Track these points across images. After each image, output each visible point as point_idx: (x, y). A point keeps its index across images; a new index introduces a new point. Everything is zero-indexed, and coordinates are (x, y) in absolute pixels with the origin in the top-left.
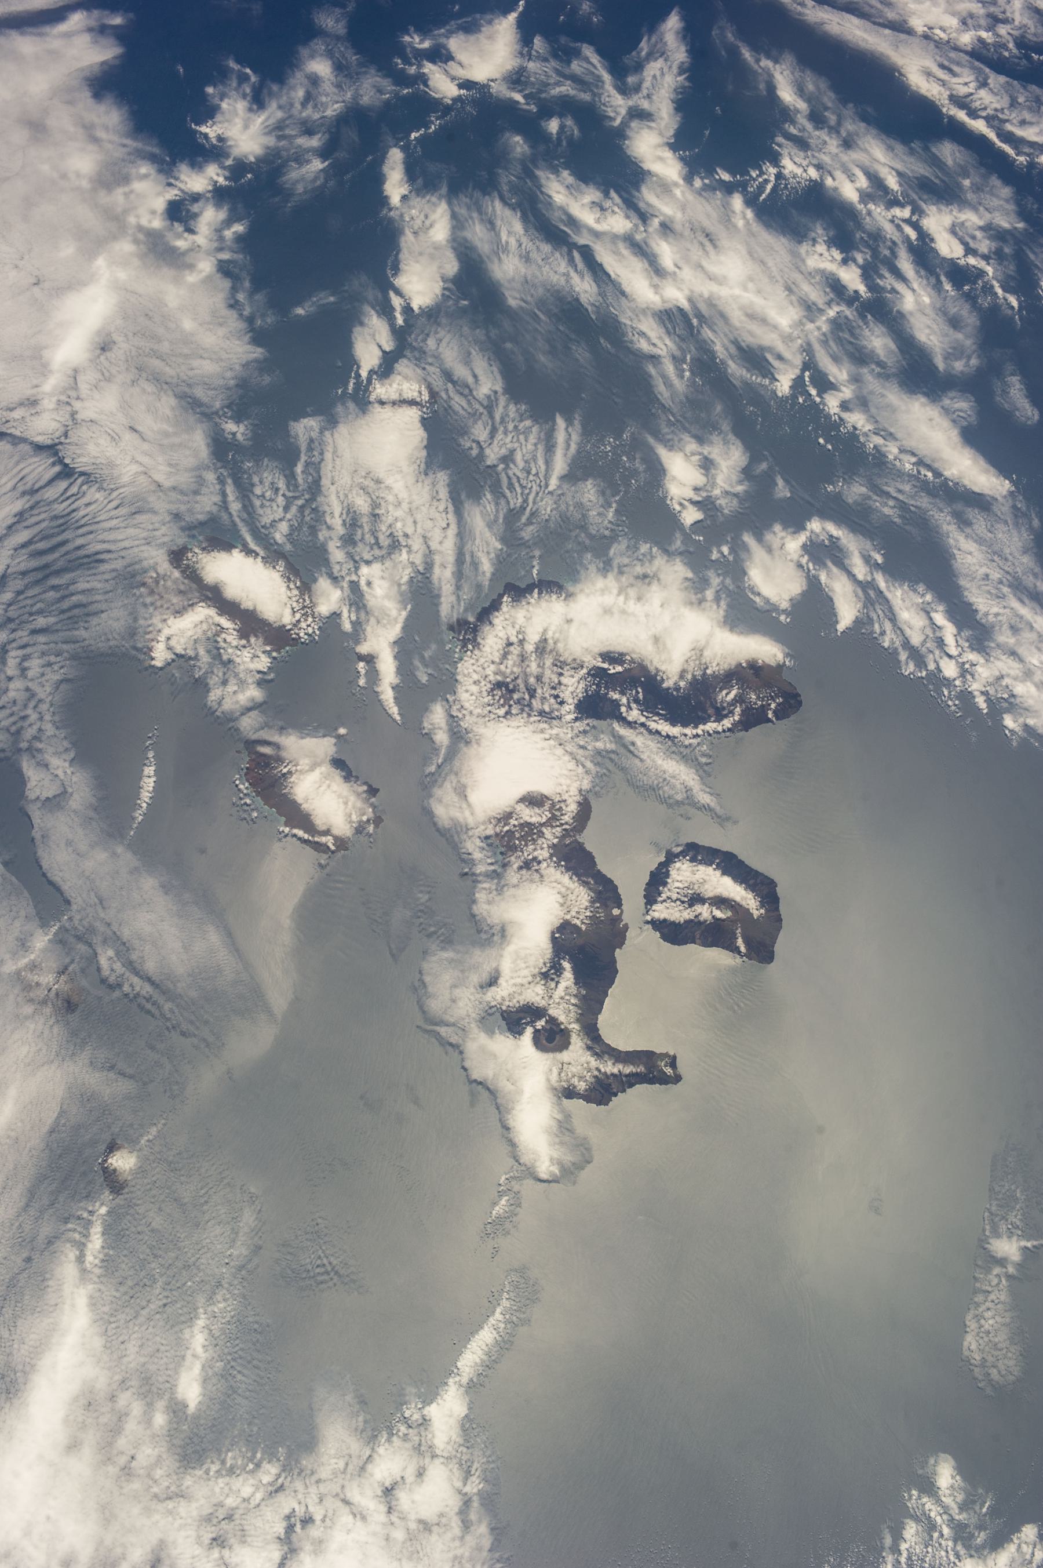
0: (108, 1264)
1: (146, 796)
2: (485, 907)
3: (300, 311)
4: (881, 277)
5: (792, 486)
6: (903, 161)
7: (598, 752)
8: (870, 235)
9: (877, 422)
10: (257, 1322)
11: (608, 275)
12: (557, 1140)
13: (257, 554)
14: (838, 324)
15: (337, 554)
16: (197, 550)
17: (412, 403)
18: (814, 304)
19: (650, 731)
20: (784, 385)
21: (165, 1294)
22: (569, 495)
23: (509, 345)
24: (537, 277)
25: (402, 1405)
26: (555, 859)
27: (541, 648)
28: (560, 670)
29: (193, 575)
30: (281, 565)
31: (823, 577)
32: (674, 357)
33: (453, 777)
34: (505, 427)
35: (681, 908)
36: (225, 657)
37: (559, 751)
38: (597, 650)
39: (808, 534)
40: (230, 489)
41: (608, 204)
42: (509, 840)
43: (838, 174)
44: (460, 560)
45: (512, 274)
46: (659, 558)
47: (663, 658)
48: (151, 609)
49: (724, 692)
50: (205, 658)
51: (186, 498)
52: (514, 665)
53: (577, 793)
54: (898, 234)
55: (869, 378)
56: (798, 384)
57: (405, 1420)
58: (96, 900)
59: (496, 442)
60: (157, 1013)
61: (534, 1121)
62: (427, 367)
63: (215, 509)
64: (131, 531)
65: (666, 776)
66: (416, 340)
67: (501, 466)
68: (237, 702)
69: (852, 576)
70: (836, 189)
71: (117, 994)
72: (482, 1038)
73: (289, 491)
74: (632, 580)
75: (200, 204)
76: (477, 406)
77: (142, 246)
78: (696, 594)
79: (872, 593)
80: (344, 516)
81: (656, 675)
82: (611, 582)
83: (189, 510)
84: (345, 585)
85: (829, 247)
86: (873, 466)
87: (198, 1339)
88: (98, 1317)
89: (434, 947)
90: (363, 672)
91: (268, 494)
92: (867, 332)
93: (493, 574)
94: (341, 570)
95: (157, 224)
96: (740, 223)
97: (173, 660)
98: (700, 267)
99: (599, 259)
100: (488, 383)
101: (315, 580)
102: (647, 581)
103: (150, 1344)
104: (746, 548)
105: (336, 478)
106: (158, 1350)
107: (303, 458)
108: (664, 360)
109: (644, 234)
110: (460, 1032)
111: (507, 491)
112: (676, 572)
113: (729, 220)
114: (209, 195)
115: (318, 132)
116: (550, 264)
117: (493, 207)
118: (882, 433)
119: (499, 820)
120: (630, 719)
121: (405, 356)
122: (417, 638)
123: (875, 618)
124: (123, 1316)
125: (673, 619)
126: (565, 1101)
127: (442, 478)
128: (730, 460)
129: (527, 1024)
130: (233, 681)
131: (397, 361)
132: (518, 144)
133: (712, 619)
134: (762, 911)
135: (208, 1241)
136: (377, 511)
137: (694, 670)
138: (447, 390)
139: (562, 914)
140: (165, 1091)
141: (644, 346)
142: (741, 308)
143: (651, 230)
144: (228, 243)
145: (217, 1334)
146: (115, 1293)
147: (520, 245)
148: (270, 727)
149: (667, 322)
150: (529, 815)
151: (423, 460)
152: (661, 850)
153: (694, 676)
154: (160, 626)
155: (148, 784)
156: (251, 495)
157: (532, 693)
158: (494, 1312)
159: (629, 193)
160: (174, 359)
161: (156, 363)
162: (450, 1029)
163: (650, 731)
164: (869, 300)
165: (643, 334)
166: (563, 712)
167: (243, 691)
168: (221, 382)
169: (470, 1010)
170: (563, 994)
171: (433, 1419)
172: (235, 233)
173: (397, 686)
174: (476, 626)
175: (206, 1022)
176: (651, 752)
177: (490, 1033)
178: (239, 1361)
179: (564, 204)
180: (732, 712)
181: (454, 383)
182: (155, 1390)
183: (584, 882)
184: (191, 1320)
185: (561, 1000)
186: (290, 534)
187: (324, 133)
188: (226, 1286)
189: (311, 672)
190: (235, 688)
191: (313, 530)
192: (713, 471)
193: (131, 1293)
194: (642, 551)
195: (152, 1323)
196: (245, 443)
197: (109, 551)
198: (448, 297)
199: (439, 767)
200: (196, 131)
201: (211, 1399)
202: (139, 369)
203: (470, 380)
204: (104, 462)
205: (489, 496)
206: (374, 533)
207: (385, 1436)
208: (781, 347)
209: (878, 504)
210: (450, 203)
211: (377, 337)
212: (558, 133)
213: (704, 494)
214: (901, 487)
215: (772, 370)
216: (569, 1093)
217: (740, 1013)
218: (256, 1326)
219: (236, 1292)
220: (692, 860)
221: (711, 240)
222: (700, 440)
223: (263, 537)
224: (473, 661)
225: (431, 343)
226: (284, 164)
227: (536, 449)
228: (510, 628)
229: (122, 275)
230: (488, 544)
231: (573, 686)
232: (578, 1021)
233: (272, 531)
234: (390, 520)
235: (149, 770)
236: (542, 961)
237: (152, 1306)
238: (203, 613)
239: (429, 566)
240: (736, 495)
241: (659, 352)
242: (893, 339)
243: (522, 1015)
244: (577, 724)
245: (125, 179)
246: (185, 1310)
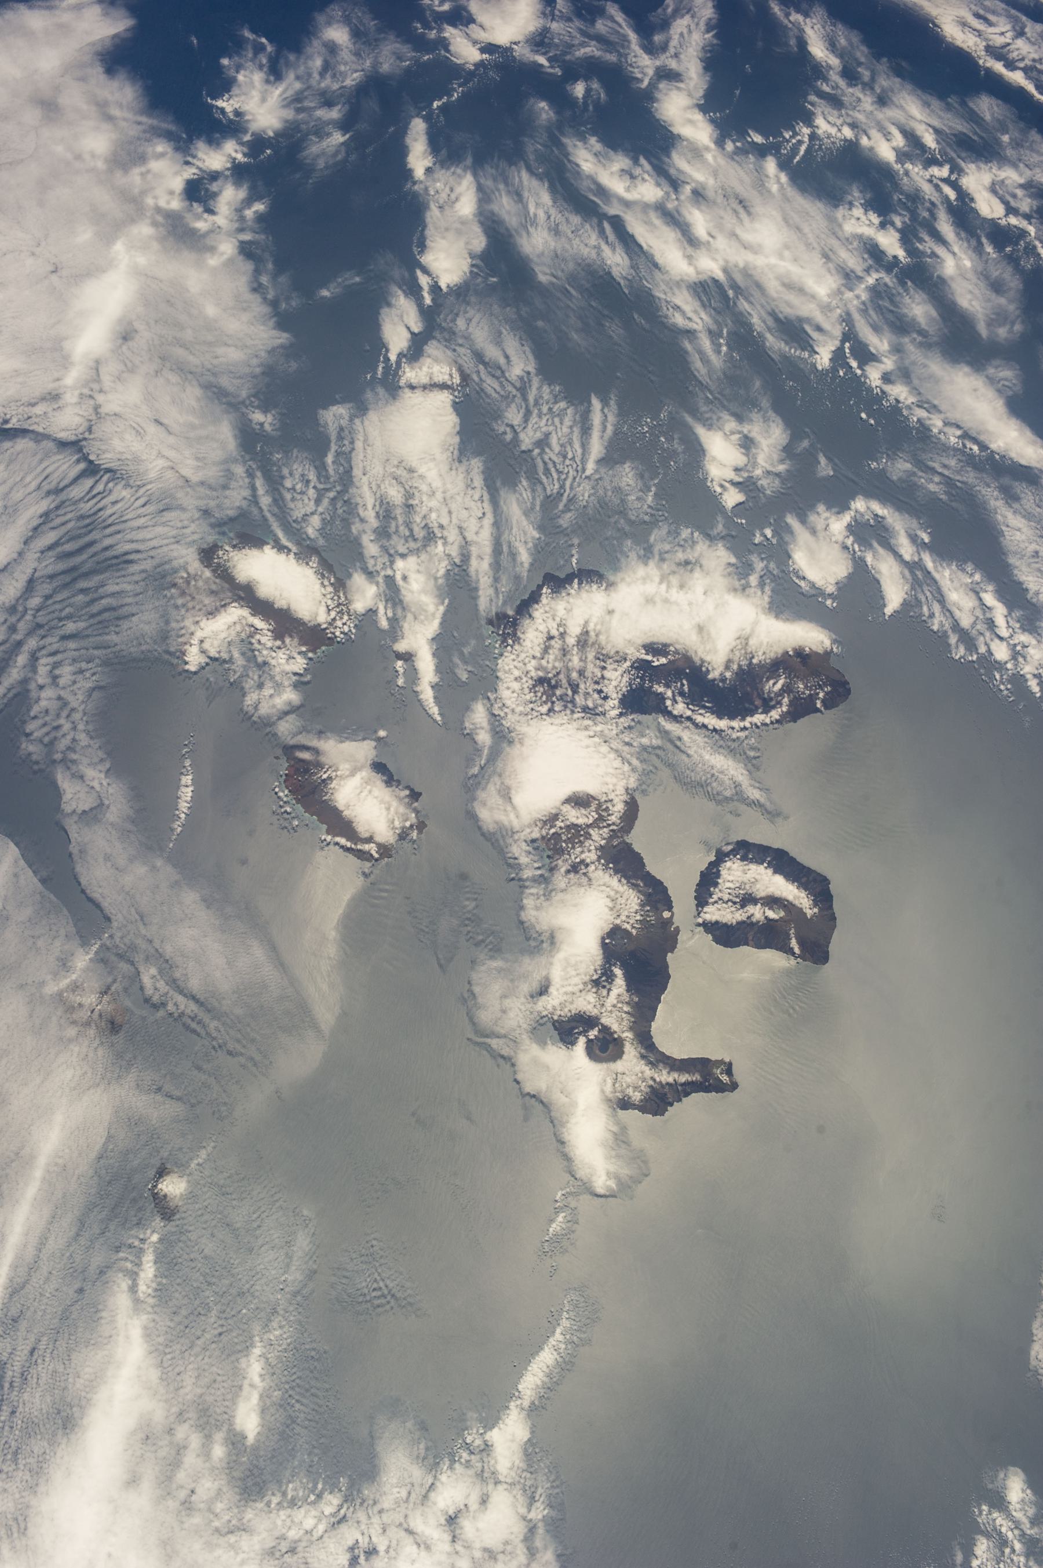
0: (161, 1293)
1: (184, 806)
2: (533, 913)
3: (325, 293)
4: (921, 240)
5: (836, 464)
6: (940, 117)
7: (644, 748)
8: (908, 196)
9: (920, 394)
10: (314, 1349)
11: (640, 247)
12: (613, 1153)
13: (290, 550)
14: (877, 292)
15: (371, 549)
16: (227, 548)
17: (443, 386)
18: (852, 271)
19: (697, 725)
20: (823, 358)
21: (220, 1322)
22: (607, 479)
23: (540, 323)
24: (567, 251)
25: (464, 1430)
26: (603, 861)
27: (583, 641)
28: (602, 664)
29: (224, 574)
30: (314, 562)
31: (869, 559)
32: (710, 332)
33: (496, 779)
34: (539, 410)
35: (733, 909)
36: (260, 660)
37: (604, 749)
38: (639, 642)
39: (852, 513)
40: (259, 483)
41: (637, 171)
42: (556, 842)
43: (874, 133)
45: (541, 248)
46: (701, 543)
47: (708, 648)
48: (183, 611)
49: (771, 682)
50: (239, 661)
51: (214, 493)
52: (556, 659)
53: (623, 791)
54: (936, 194)
55: (911, 348)
56: (838, 356)
57: (467, 1447)
58: (137, 917)
59: (530, 426)
60: (203, 1033)
61: (589, 1134)
62: (457, 348)
63: (244, 504)
64: (160, 530)
65: (714, 771)
66: (445, 320)
68: (274, 706)
69: (898, 556)
70: (871, 149)
71: (161, 1013)
72: (535, 1050)
73: (321, 483)
74: (674, 568)
75: (219, 182)
76: (510, 388)
77: (161, 229)
78: (739, 580)
79: (919, 573)
81: (701, 666)
82: (652, 570)
84: (380, 580)
85: (866, 210)
86: (916, 439)
87: (254, 1368)
88: (153, 1348)
89: (482, 956)
90: (401, 670)
91: (299, 487)
92: (907, 300)
93: (531, 565)
94: (375, 565)
95: (176, 204)
96: (775, 188)
97: (207, 664)
98: (734, 235)
99: (630, 229)
100: (520, 364)
101: (350, 576)
102: (689, 567)
103: (207, 1374)
105: (368, 468)
106: (215, 1381)
107: (334, 447)
108: (700, 335)
109: (676, 203)
110: (511, 1044)
111: (543, 477)
112: (718, 557)
113: (763, 185)
114: (228, 173)
115: (338, 104)
116: (580, 236)
117: (520, 178)
118: (926, 405)
119: (545, 823)
120: (675, 712)
121: (434, 338)
122: (456, 634)
123: (923, 600)
124: (179, 1346)
125: (717, 607)
126: (620, 1112)
127: (477, 464)
128: (771, 437)
129: (580, 1034)
130: (269, 684)
131: (426, 343)
132: (543, 110)
133: (757, 606)
134: (816, 910)
135: (262, 1266)
136: (411, 502)
137: (740, 660)
138: (478, 372)
139: (612, 918)
140: (214, 1113)
141: (679, 320)
142: (778, 278)
143: (682, 197)
144: (250, 223)
145: (273, 1362)
146: (169, 1323)
147: (549, 217)
148: (308, 732)
149: (702, 295)
150: (576, 816)
151: (457, 447)
152: (709, 851)
153: (740, 666)
154: (192, 628)
155: (186, 793)
156: (281, 489)
158: (554, 1332)
159: (659, 159)
161: (180, 352)
162: (501, 1041)
163: (697, 725)
164: (908, 265)
165: (677, 308)
166: (607, 708)
167: (279, 695)
168: (247, 370)
169: (521, 1021)
170: (615, 1002)
171: (495, 1445)
172: (256, 212)
173: (436, 684)
174: (515, 620)
175: (253, 1041)
176: (698, 747)
177: (542, 1043)
178: (297, 1389)
179: (592, 172)
180: (780, 703)
181: (486, 364)
182: (213, 1422)
183: (633, 884)
184: (247, 1349)
185: (613, 1007)
186: (323, 529)
187: (344, 104)
188: (282, 1312)
189: (347, 669)
190: (272, 691)
191: (347, 523)
192: (754, 451)
193: (186, 1322)
194: (684, 536)
195: (208, 1353)
196: (274, 433)
197: (138, 551)
198: (477, 274)
199: (482, 768)
200: (213, 106)
201: (270, 1430)
202: (163, 358)
203: (502, 361)
204: (129, 457)
205: (525, 483)
206: (408, 525)
207: (447, 1463)
208: (819, 318)
209: (923, 480)
210: (475, 175)
211: (405, 317)
212: (584, 97)
213: (746, 475)
214: (946, 462)
216: (624, 1104)
217: (795, 1015)
218: (313, 1353)
219: (292, 1318)
220: (743, 859)
221: (745, 207)
222: (740, 418)
223: (294, 530)
225: (461, 323)
226: (304, 138)
227: (572, 432)
228: (550, 621)
229: (142, 260)
230: (525, 533)
231: (617, 680)
232: (631, 1029)
233: (304, 525)
234: (424, 510)
236: (593, 968)
237: (207, 1336)
238: (236, 614)
239: (466, 557)
241: (695, 326)
242: (934, 306)
243: (574, 1024)
244: (622, 720)
245: (142, 159)
246: (241, 1338)
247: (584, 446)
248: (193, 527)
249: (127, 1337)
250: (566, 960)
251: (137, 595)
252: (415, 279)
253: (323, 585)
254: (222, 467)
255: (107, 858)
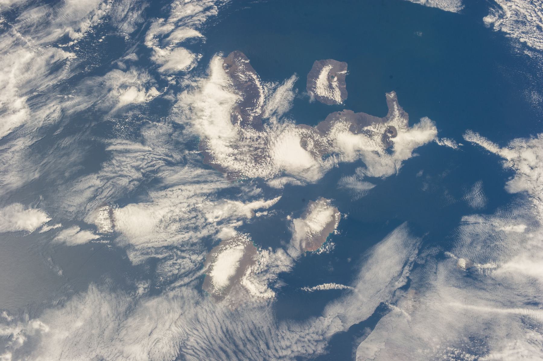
0: (494, 260)
13: (210, 265)
15: (204, 233)
17: (111, 213)
20: (71, 55)
23: (67, 174)
27: (236, 147)
29: (226, 290)
31: (177, 41)
32: (61, 102)
34: (119, 171)
36: (266, 268)
37: (281, 136)
38: (232, 126)
40: (177, 284)
44: (198, 182)
50: (268, 276)
56: (66, 49)
59: (128, 174)
64: (209, 321)
67: (142, 170)
68: (285, 259)
71: (411, 278)
74: (194, 114)
76: (108, 184)
78: (195, 89)
80: (183, 233)
83: (193, 298)
84: (219, 227)
91: (177, 267)
93: (202, 168)
100: (94, 181)
102: (192, 108)
104: (166, 71)
105: (163, 239)
107: (153, 256)
111: (156, 167)
120: (261, 112)
127: (153, 194)
128: (117, 77)
130: (276, 263)
131: (86, 223)
136: (178, 219)
141: (56, 115)
149: (38, 106)
153: (236, 89)
154: (256, 298)
156: (179, 274)
157: (256, 149)
160: (103, 325)
162: (397, 165)
163: (265, 104)
165: (48, 116)
180: (250, 75)
181: (95, 197)
186: (197, 253)
190: (279, 261)
191: (193, 244)
192: (127, 84)
197: (221, 327)
203: (92, 189)
205: (160, 174)
206: (190, 219)
213: (141, 87)
215: (61, 60)
220: (315, 88)
222: (110, 90)
223: (201, 265)
224: (247, 172)
225: (71, 209)
228: (228, 160)
231: (250, 133)
232: (384, 124)
235: (322, 287)
238: (245, 282)
239: (203, 195)
240: (139, 74)
244: (268, 131)
247: (136, 151)
248: (204, 307)
249: (508, 268)
250: (364, 146)
251: (243, 323)
252: (45, 232)
253: (226, 248)
254: (172, 301)
255: (359, 309)
